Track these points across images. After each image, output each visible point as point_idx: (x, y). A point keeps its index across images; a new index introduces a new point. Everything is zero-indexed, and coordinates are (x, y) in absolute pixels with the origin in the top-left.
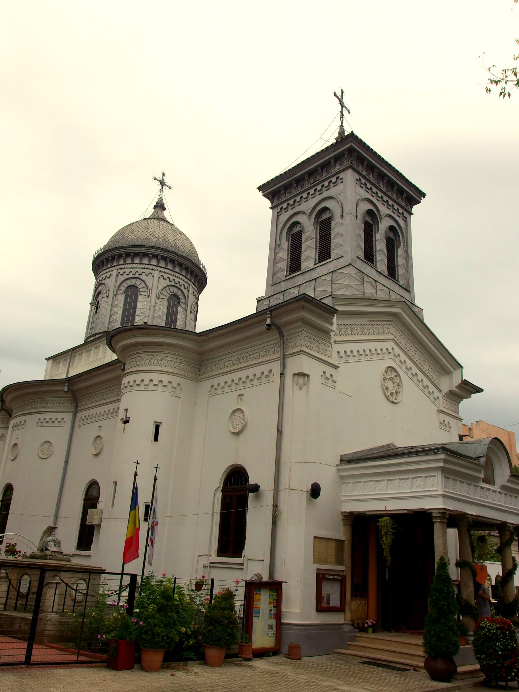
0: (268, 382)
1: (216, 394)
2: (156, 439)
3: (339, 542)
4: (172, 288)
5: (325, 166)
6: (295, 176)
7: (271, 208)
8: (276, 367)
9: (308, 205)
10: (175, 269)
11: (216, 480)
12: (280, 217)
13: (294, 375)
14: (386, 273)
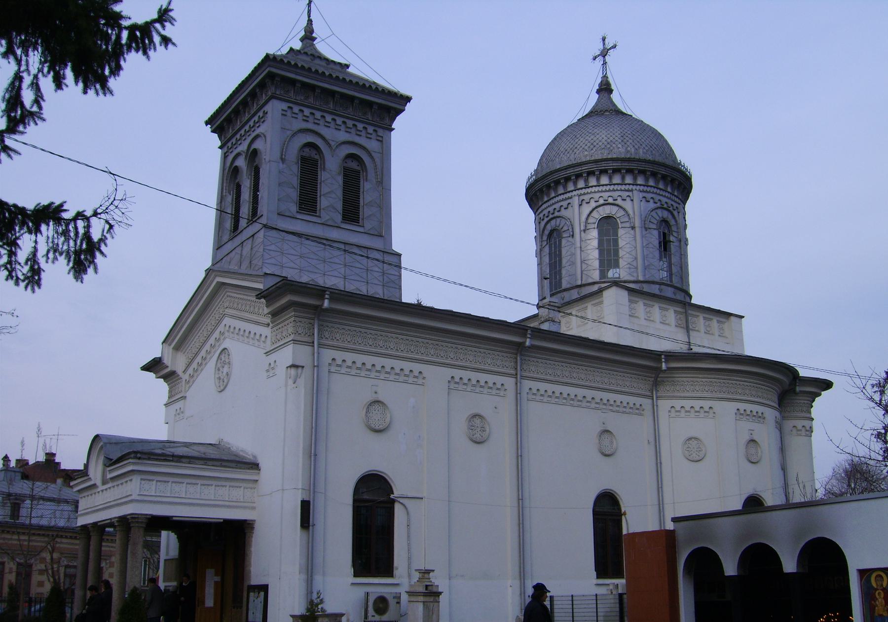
4: (659, 212)
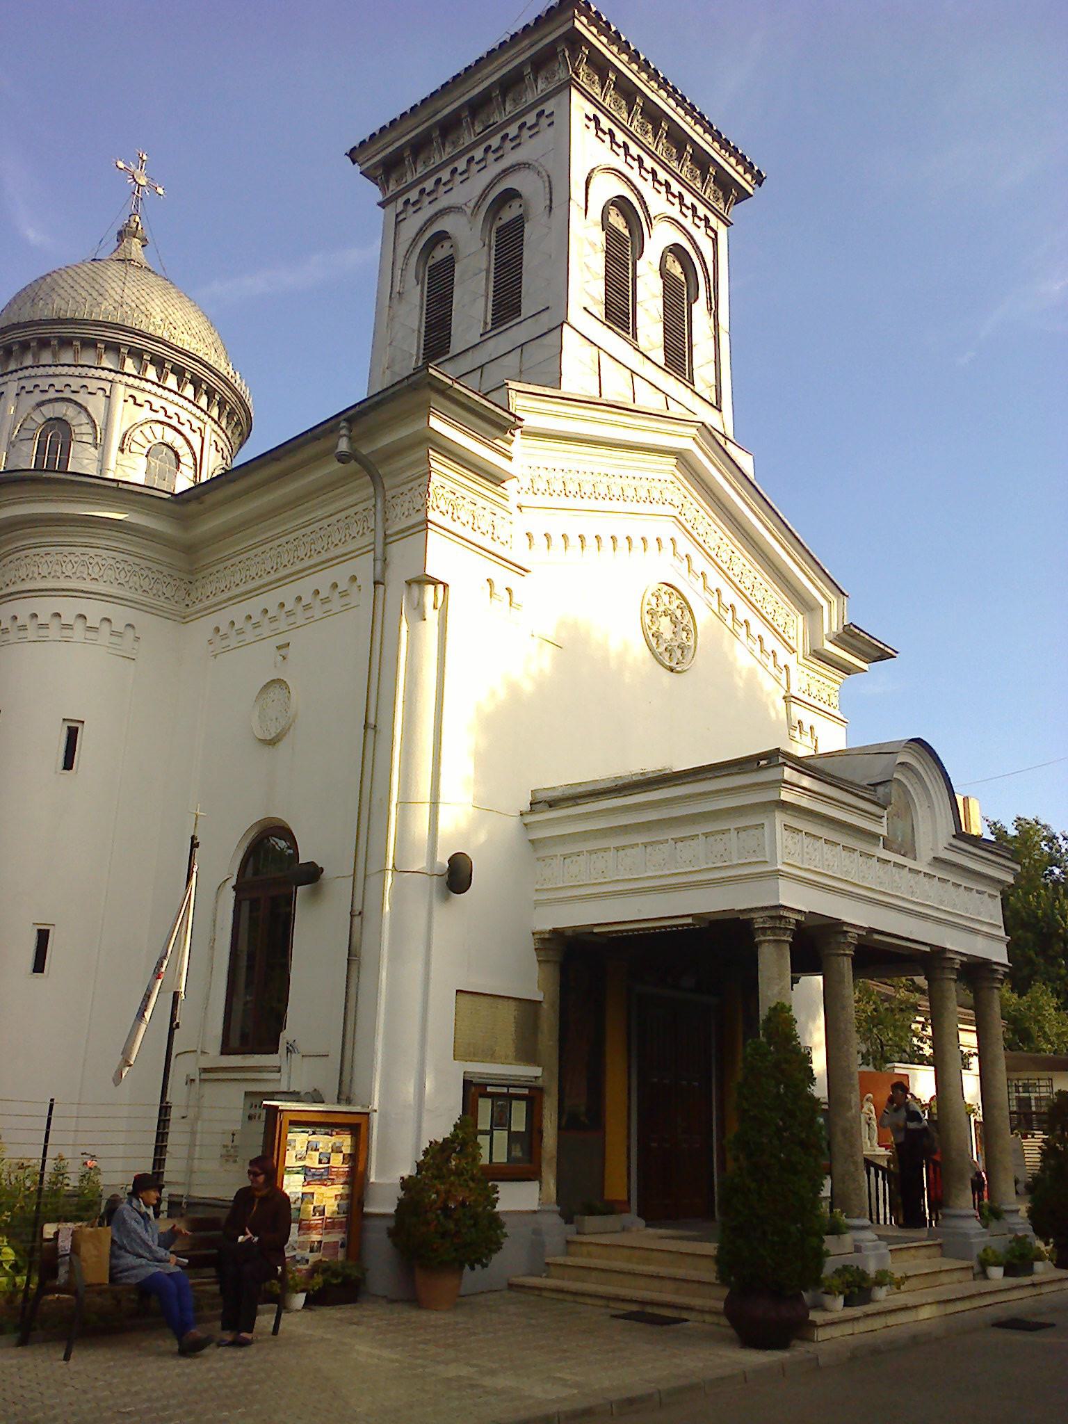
0: (347, 608)
1: (227, 649)
2: (68, 764)
3: (528, 1007)
5: (511, 84)
6: (439, 117)
7: (382, 205)
8: (364, 567)
9: (468, 191)
10: (165, 379)
11: (222, 861)
12: (402, 224)
13: (409, 583)
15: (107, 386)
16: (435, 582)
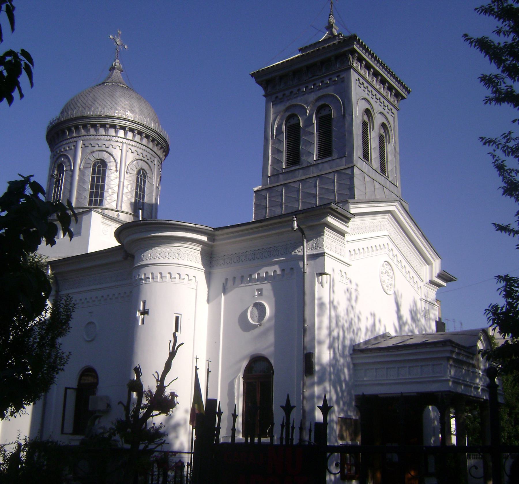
7: (263, 96)
14: (379, 170)
15: (120, 145)
16: (326, 274)
